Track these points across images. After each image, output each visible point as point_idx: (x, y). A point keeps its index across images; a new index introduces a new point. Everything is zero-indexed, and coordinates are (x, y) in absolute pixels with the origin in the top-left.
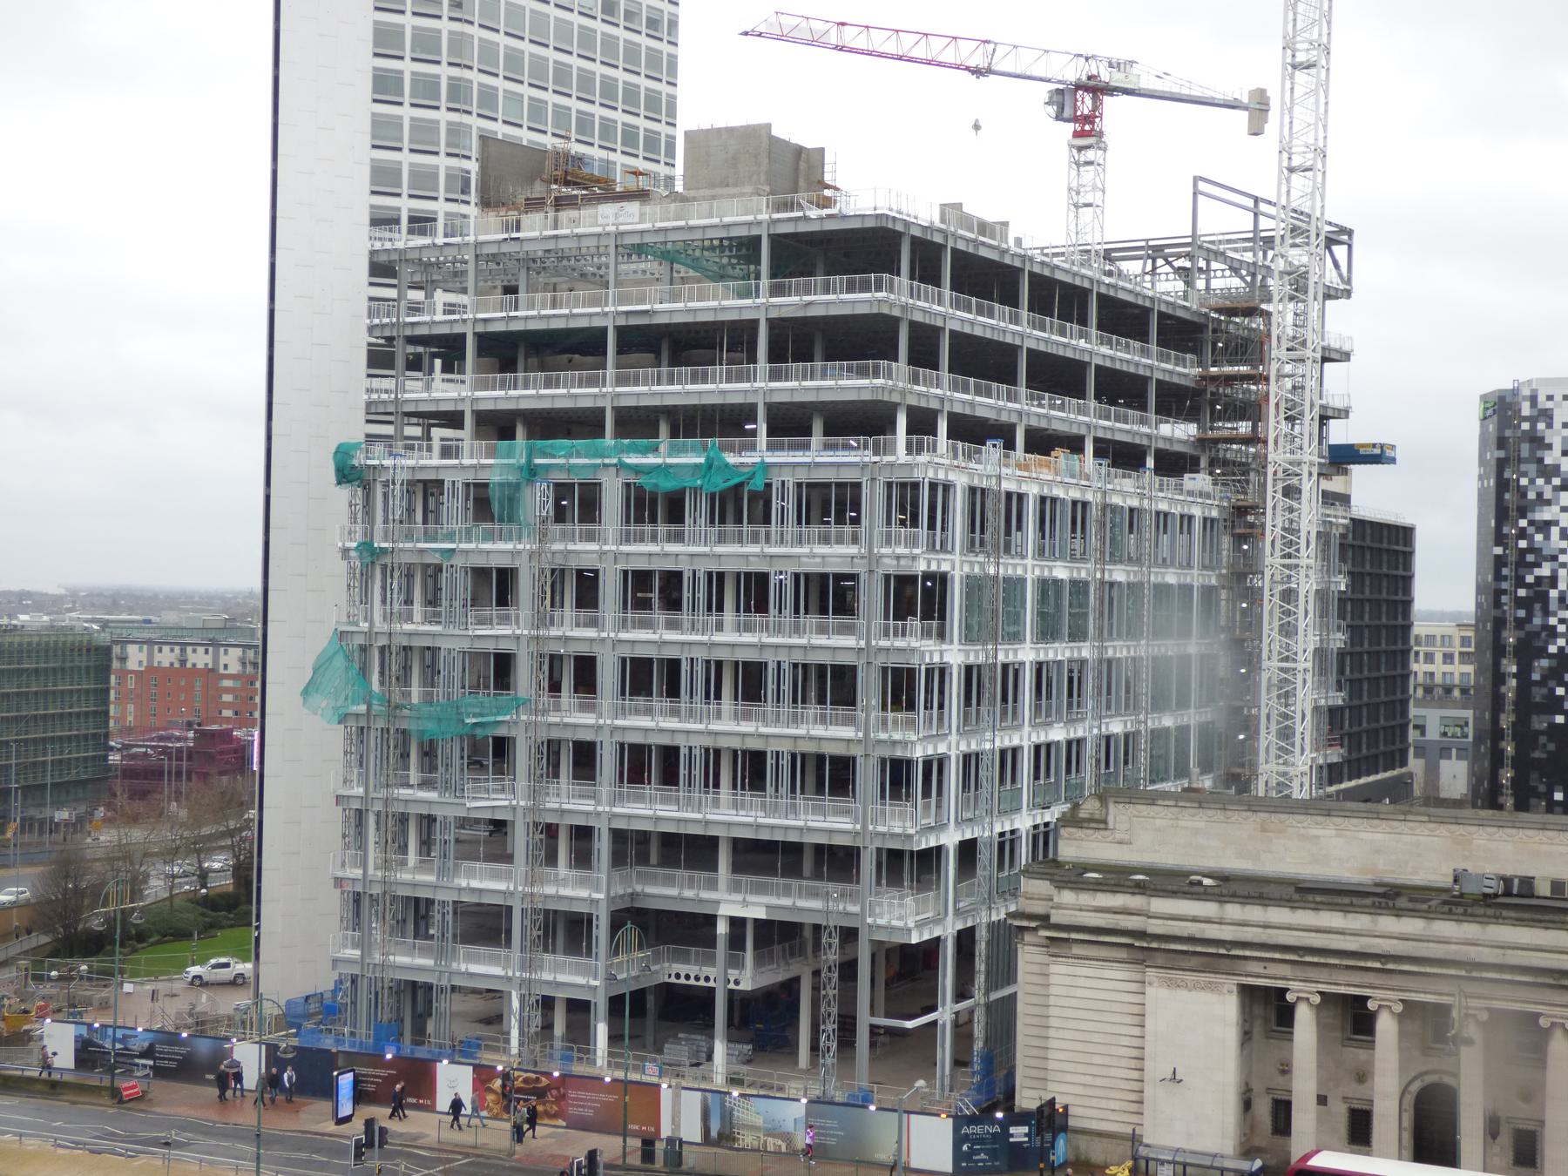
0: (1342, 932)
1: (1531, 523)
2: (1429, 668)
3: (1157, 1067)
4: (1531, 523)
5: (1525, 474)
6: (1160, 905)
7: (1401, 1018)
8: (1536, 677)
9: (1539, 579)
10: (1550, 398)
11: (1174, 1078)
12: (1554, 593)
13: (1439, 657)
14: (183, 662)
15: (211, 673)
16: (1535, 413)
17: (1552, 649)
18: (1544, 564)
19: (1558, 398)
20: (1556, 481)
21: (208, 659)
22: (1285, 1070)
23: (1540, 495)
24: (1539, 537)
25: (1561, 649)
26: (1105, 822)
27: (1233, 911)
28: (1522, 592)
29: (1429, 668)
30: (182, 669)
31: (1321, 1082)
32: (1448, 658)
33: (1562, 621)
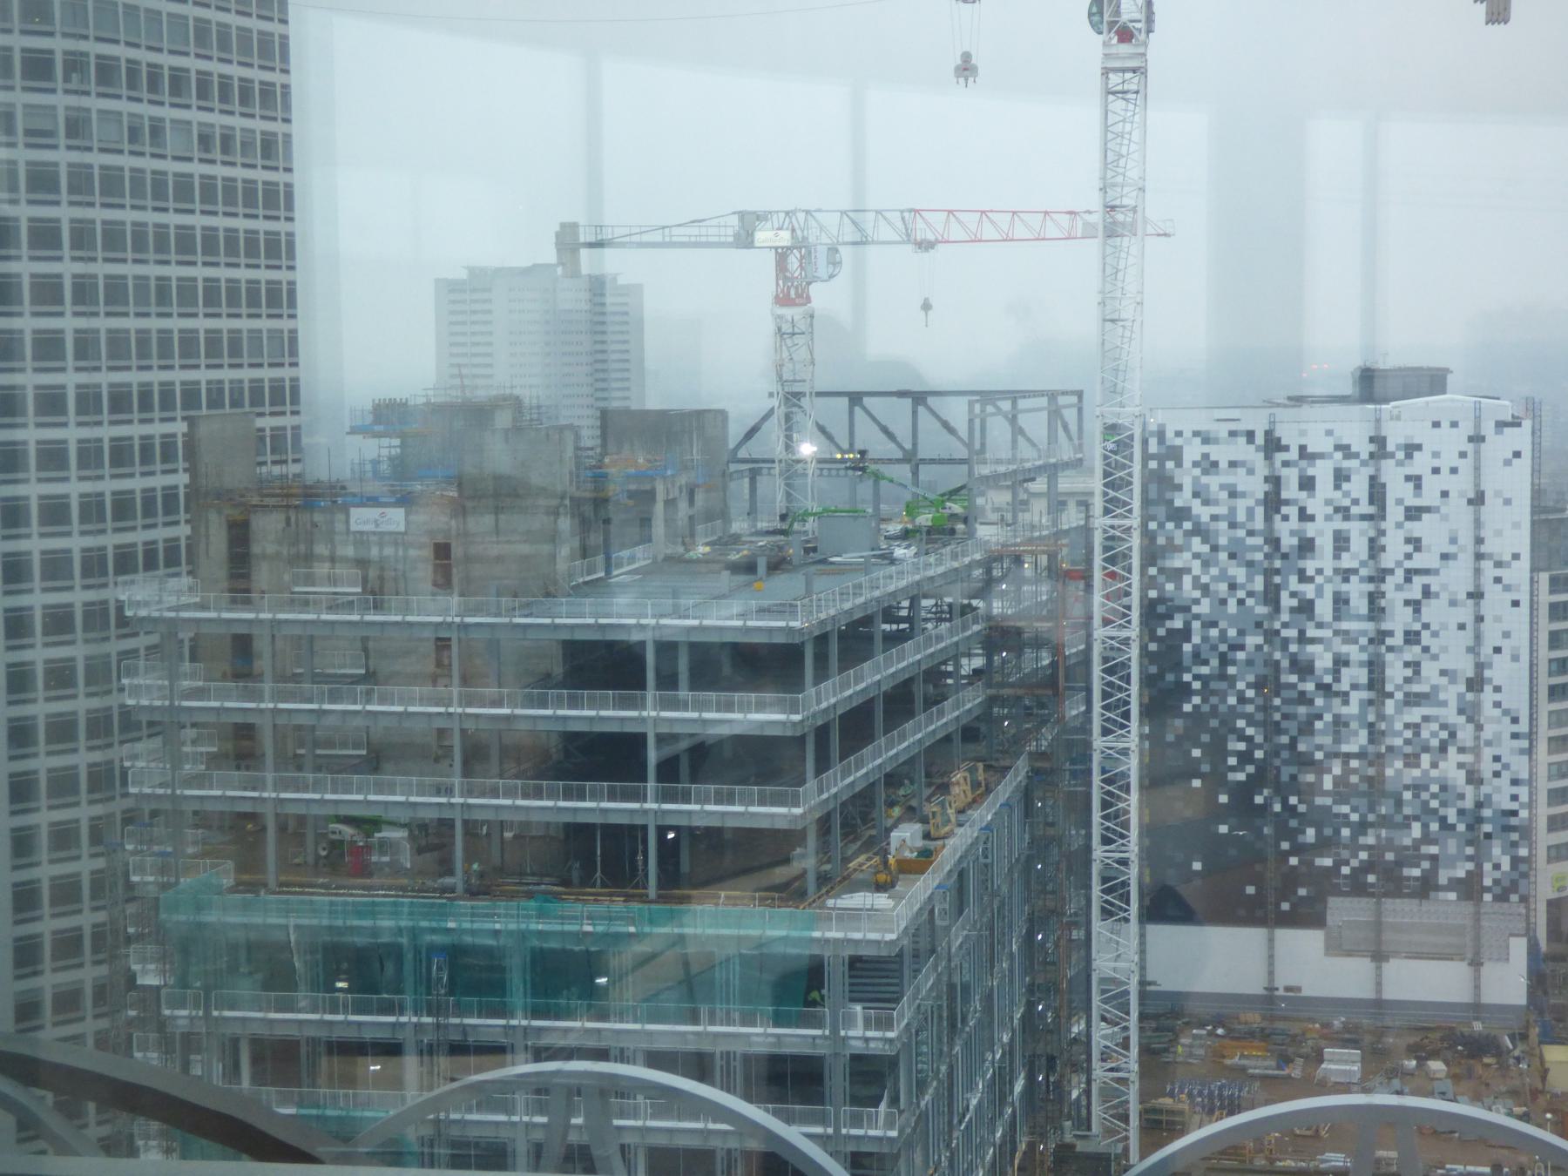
1: (1161, 571)
4: (1161, 571)
5: (1153, 518)
8: (1170, 738)
9: (1170, 632)
10: (1179, 434)
12: (1187, 647)
16: (1163, 451)
17: (1187, 708)
18: (1176, 616)
19: (1188, 434)
20: (1187, 525)
23: (1170, 539)
24: (1170, 587)
25: (1195, 707)
28: (1153, 647)
33: (1196, 677)
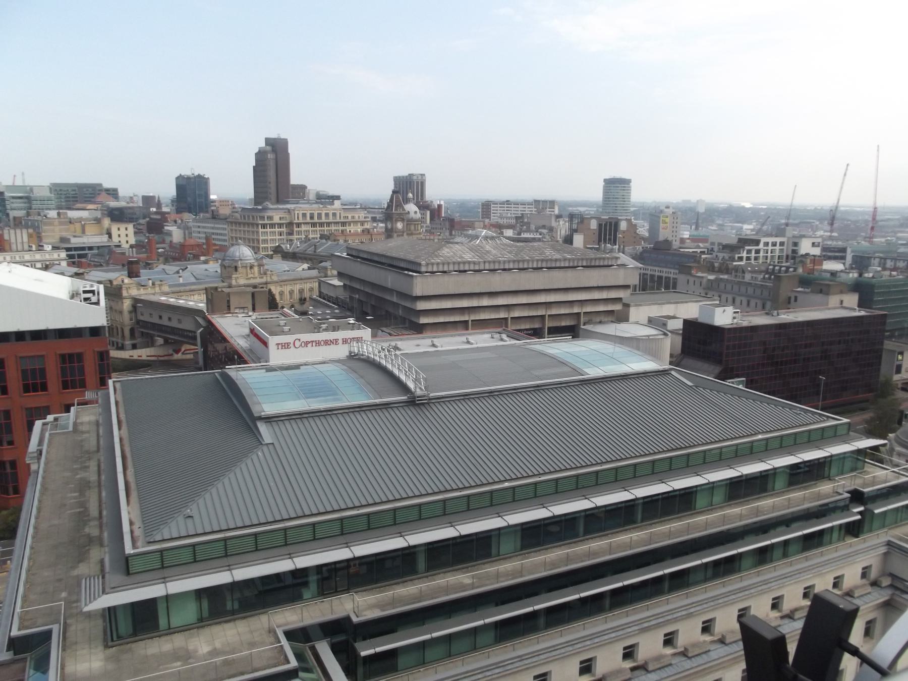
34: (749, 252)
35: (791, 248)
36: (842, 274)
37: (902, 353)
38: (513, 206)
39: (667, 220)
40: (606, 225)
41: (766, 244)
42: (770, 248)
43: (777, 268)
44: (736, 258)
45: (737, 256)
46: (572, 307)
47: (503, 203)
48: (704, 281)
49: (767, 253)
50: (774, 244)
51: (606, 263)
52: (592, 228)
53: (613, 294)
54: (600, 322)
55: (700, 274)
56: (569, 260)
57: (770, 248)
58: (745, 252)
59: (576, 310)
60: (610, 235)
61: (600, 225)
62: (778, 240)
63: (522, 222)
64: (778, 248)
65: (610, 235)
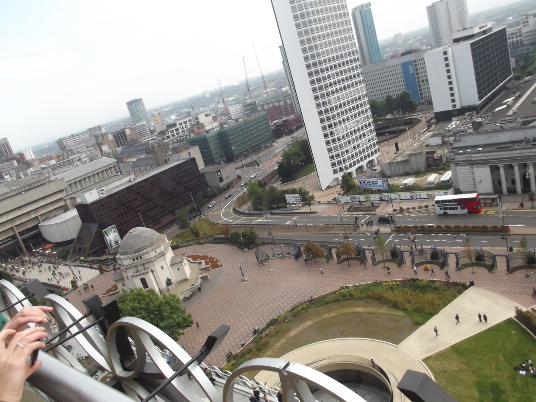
0: (506, 155)
2: (513, 40)
3: (477, 180)
6: (473, 155)
7: (518, 166)
11: (481, 182)
13: (515, 37)
14: (274, 105)
15: (279, 106)
21: (278, 104)
22: (499, 175)
26: (460, 140)
27: (487, 154)
29: (513, 40)
30: (274, 108)
31: (506, 176)
32: (517, 37)
34: (172, 132)
35: (196, 121)
36: (211, 130)
37: (219, 171)
38: (76, 137)
39: (157, 119)
40: (118, 135)
41: (181, 124)
42: (184, 125)
43: (182, 138)
44: (166, 138)
45: (165, 137)
46: (30, 215)
47: (69, 137)
48: (131, 163)
49: (183, 128)
50: (185, 123)
51: (42, 183)
52: (110, 139)
53: (59, 196)
54: (55, 216)
55: (129, 160)
56: (15, 190)
57: (184, 125)
58: (170, 133)
59: (33, 216)
60: (123, 139)
61: (115, 136)
62: (187, 119)
63: (66, 150)
64: (188, 123)
65: (123, 139)
